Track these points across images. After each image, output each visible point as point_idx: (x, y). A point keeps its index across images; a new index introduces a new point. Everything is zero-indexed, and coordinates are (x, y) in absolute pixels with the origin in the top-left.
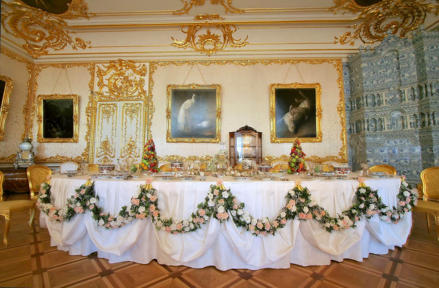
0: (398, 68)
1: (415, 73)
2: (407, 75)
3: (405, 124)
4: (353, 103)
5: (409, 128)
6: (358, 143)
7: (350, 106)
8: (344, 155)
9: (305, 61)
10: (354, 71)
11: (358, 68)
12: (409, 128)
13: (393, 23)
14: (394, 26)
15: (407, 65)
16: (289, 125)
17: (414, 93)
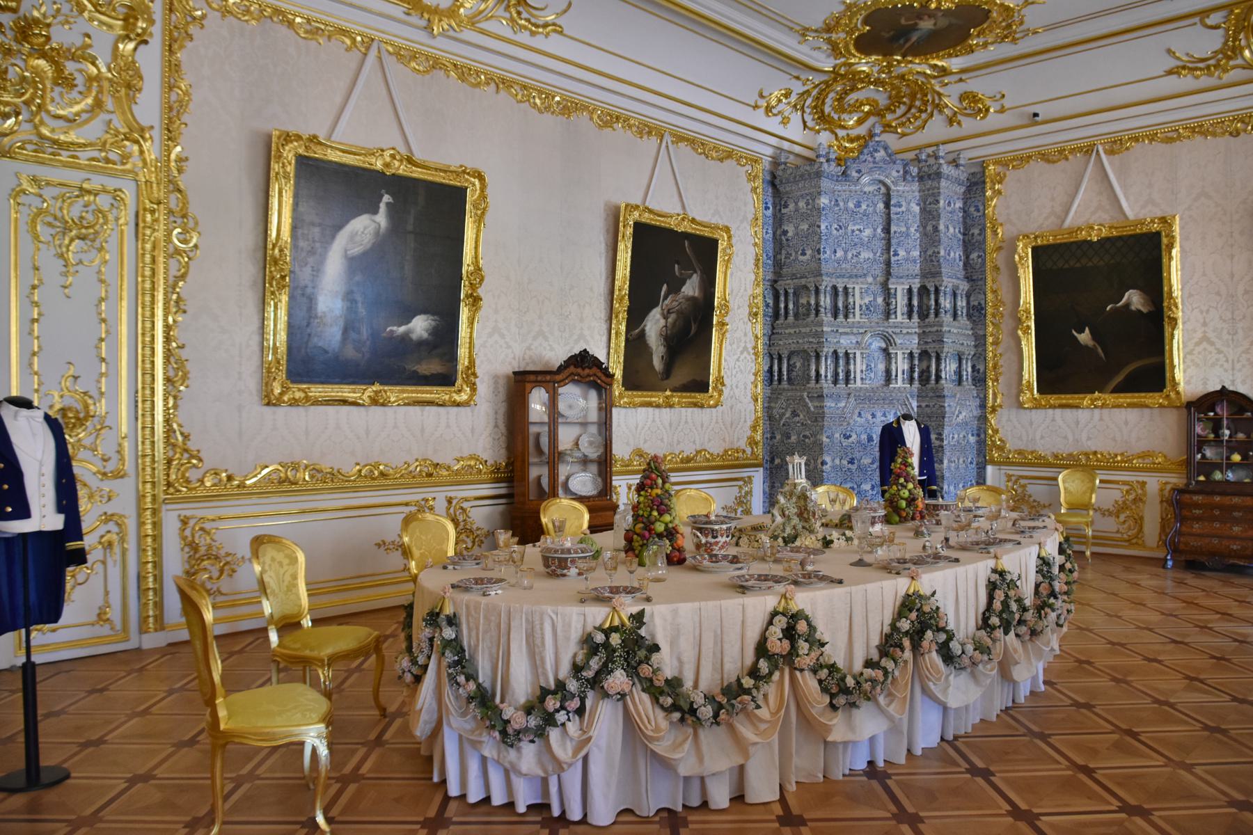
0: (887, 230)
1: (916, 253)
2: (902, 253)
3: (894, 373)
4: (782, 298)
5: (900, 383)
6: (795, 414)
7: (771, 302)
8: (756, 443)
9: (692, 142)
10: (792, 206)
11: (807, 204)
12: (900, 383)
13: (868, 102)
14: (867, 108)
15: (904, 229)
16: (654, 348)
17: (910, 299)
